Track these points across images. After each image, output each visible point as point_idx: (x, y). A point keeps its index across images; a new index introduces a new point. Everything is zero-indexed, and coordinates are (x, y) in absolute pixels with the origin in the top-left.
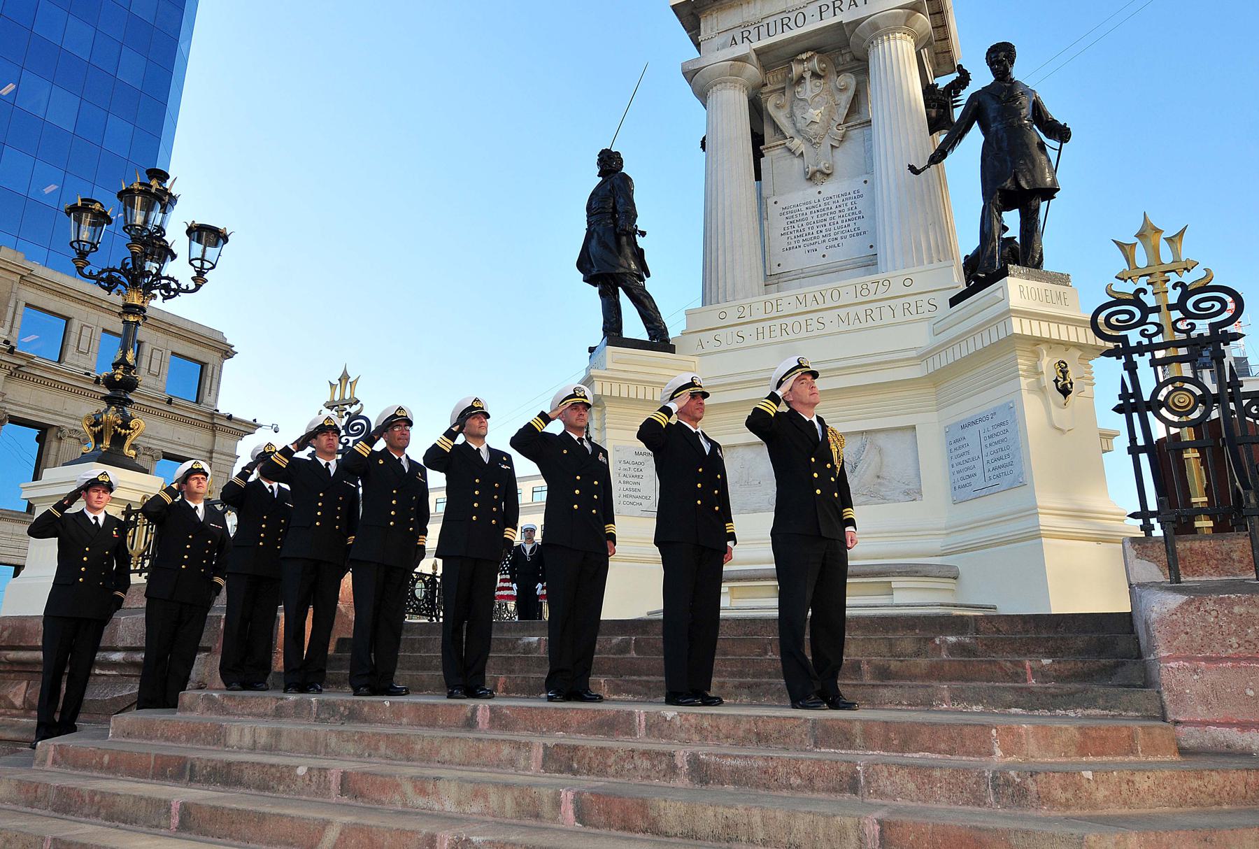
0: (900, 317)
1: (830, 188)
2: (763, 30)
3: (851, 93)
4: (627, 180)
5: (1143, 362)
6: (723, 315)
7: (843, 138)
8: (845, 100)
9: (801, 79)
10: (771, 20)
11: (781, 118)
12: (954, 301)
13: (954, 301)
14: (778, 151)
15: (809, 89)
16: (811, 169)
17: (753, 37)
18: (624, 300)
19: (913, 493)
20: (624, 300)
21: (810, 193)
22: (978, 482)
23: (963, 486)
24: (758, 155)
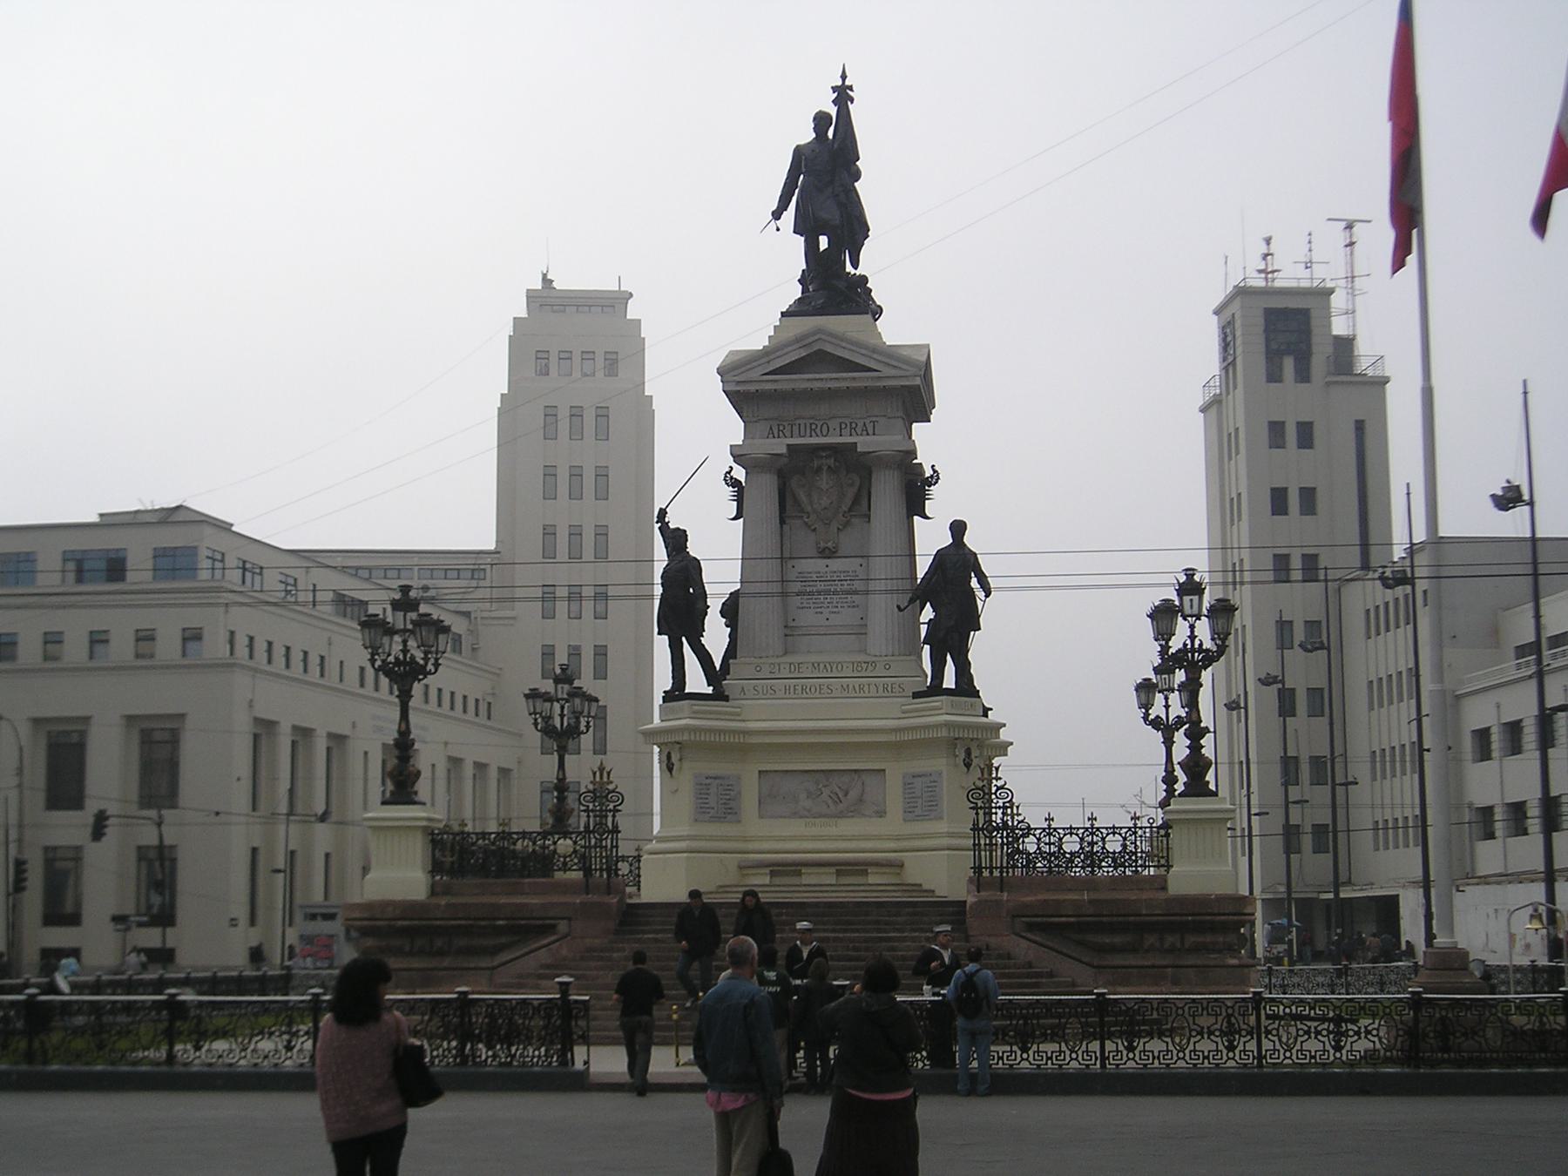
0: (881, 693)
1: (836, 564)
2: (796, 428)
3: (855, 489)
4: (696, 565)
5: (981, 812)
6: (759, 668)
7: (847, 524)
8: (850, 493)
9: (819, 470)
10: (802, 422)
11: (803, 497)
12: (916, 695)
13: (916, 695)
14: (798, 522)
15: (824, 481)
16: (822, 545)
17: (788, 434)
18: (686, 648)
19: (881, 814)
20: (686, 648)
21: (820, 564)
22: (918, 811)
23: (910, 813)
24: (782, 522)
